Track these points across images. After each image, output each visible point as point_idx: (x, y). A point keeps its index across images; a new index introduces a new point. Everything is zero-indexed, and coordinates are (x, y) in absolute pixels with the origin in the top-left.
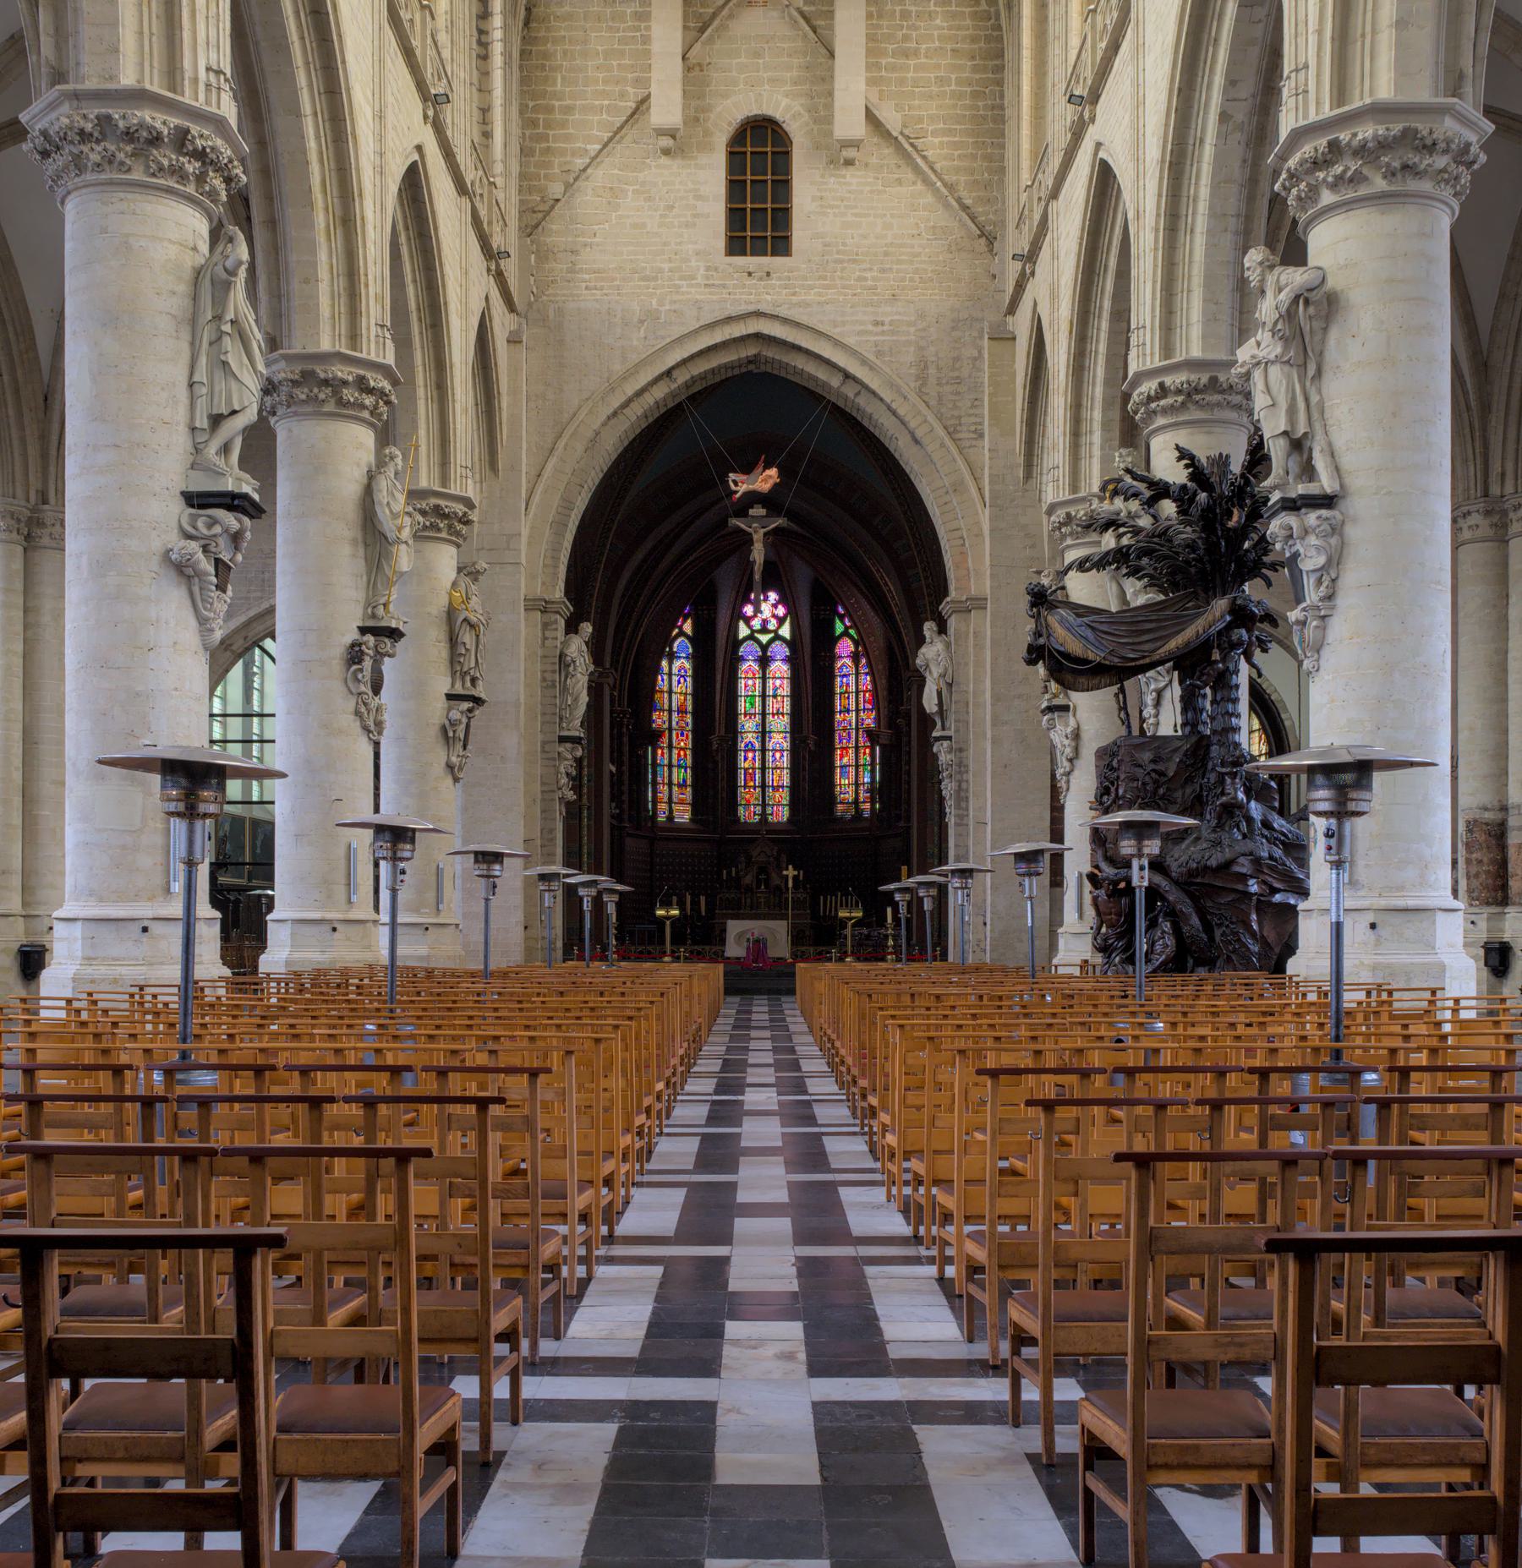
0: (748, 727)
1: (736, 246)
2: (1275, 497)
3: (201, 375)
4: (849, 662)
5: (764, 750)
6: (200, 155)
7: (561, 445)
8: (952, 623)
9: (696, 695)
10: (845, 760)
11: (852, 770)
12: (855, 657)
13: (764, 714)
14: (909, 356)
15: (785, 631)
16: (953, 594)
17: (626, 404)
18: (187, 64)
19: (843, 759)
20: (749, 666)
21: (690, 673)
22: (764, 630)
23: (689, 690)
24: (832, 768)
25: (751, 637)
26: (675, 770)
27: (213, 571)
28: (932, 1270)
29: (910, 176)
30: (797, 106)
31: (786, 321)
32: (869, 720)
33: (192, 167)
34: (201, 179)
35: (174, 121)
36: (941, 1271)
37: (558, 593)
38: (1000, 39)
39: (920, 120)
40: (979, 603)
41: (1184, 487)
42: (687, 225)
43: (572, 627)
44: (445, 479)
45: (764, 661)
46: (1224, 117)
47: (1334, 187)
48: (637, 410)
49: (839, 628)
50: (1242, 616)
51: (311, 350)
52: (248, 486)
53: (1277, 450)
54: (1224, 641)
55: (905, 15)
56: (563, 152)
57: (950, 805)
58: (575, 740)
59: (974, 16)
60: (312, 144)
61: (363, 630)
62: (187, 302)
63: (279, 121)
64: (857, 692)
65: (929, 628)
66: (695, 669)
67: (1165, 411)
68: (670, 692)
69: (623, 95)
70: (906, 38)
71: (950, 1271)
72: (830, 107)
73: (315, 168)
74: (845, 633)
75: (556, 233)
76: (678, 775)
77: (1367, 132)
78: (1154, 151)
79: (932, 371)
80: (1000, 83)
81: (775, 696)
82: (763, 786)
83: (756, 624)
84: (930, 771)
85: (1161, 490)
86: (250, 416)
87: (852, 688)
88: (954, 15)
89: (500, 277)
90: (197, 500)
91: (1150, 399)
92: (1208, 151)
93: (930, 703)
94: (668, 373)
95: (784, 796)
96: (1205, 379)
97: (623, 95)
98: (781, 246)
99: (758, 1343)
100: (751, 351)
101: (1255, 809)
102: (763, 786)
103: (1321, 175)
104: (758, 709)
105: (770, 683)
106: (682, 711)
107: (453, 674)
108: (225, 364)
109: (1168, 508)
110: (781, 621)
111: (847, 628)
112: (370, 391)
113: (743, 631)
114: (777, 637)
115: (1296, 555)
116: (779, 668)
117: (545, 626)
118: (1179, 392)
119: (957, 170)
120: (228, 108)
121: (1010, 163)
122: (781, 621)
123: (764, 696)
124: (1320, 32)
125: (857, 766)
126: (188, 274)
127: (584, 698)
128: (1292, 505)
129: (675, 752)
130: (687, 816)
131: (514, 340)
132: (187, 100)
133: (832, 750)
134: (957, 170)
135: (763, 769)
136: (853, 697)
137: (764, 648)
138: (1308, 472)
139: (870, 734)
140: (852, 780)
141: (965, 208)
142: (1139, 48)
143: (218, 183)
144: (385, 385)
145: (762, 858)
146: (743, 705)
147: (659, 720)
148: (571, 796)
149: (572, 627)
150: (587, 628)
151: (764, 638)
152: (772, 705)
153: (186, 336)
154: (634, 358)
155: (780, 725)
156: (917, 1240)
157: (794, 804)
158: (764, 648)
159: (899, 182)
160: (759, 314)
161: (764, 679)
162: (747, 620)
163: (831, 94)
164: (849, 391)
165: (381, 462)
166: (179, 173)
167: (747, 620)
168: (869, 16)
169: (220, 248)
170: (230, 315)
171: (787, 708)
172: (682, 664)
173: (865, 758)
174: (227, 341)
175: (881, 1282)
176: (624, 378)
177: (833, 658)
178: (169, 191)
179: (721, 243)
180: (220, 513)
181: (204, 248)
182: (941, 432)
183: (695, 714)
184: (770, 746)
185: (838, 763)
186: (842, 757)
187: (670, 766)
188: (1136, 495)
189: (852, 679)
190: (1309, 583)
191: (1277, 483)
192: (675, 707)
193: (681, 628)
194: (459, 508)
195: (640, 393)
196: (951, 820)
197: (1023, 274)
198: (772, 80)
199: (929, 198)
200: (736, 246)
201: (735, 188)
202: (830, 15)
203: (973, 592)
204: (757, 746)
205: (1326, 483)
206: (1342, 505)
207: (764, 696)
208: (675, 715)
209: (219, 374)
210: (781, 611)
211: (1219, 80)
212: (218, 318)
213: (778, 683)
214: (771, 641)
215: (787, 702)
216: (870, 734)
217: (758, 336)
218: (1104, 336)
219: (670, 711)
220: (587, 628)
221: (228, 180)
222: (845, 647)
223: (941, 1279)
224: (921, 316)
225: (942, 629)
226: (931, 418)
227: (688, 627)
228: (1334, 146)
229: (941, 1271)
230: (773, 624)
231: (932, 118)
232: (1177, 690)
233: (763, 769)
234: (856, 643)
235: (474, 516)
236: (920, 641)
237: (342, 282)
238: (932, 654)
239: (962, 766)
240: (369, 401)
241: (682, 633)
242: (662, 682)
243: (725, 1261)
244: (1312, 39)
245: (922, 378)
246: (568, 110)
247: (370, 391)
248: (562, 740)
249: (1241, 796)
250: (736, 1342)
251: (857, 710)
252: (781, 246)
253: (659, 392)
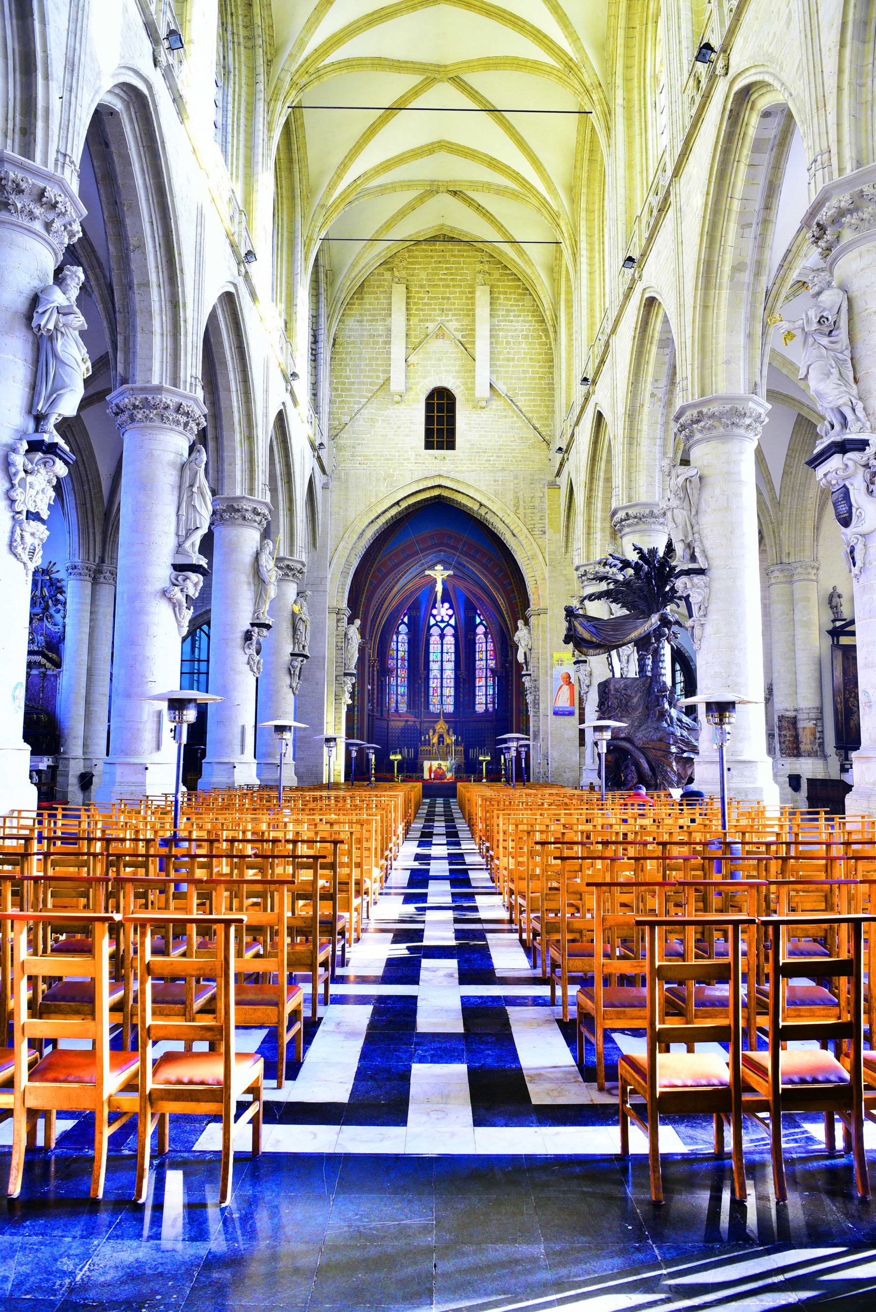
0: (434, 667)
1: (429, 446)
2: (678, 570)
3: (183, 511)
5: (442, 678)
6: (187, 414)
7: (346, 536)
8: (533, 620)
9: (409, 652)
12: (486, 634)
13: (442, 661)
14: (510, 496)
15: (452, 622)
16: (533, 607)
17: (377, 517)
18: (182, 375)
19: (480, 683)
20: (434, 639)
22: (442, 621)
24: (475, 687)
25: (436, 625)
27: (184, 600)
28: (517, 936)
29: (511, 414)
30: (458, 382)
31: (453, 480)
32: (492, 664)
33: (183, 419)
34: (186, 424)
35: (177, 400)
36: (521, 936)
37: (345, 605)
38: (552, 354)
39: (515, 389)
40: (545, 611)
41: (637, 563)
42: (407, 435)
43: (351, 621)
44: (292, 553)
45: (442, 636)
46: (653, 395)
47: (701, 431)
48: (383, 520)
49: (478, 620)
50: (665, 622)
51: (231, 496)
52: (203, 562)
53: (679, 548)
54: (658, 634)
55: (508, 343)
56: (349, 402)
57: (530, 706)
58: (351, 675)
59: (541, 344)
60: (235, 404)
61: (253, 625)
62: (177, 479)
63: (222, 394)
65: (520, 623)
66: (409, 640)
67: (629, 526)
68: (397, 650)
69: (378, 377)
70: (508, 353)
71: (525, 936)
72: (473, 383)
73: (236, 414)
74: (481, 623)
75: (345, 438)
76: (401, 690)
77: (715, 408)
78: (621, 409)
79: (521, 502)
80: (552, 373)
82: (442, 695)
83: (439, 618)
84: (522, 692)
85: (626, 564)
86: (204, 530)
88: (530, 343)
89: (319, 458)
90: (179, 568)
91: (622, 520)
92: (646, 410)
93: (521, 658)
94: (397, 503)
95: (451, 700)
96: (647, 511)
97: (378, 377)
98: (451, 446)
99: (434, 970)
100: (436, 492)
101: (674, 713)
102: (442, 695)
103: (695, 426)
104: (439, 659)
106: (403, 659)
107: (294, 644)
108: (194, 506)
109: (630, 571)
110: (450, 617)
112: (259, 514)
113: (432, 622)
114: (449, 625)
115: (689, 596)
116: (450, 640)
117: (338, 620)
118: (635, 517)
119: (532, 412)
120: (200, 394)
121: (557, 408)
122: (450, 617)
123: (442, 652)
124: (692, 365)
126: (178, 466)
127: (356, 655)
128: (688, 572)
131: (325, 487)
132: (181, 390)
133: (475, 678)
134: (532, 412)
135: (442, 687)
137: (442, 630)
138: (693, 558)
139: (492, 670)
141: (535, 428)
142: (614, 364)
143: (193, 425)
144: (267, 512)
146: (432, 657)
147: (391, 663)
148: (350, 702)
149: (351, 621)
150: (358, 622)
151: (442, 625)
153: (176, 494)
154: (381, 496)
155: (449, 666)
156: (511, 921)
157: (456, 704)
158: (442, 630)
159: (505, 417)
160: (440, 476)
161: (442, 644)
162: (434, 616)
163: (474, 377)
164: (483, 511)
165: (262, 547)
166: (178, 423)
167: (434, 616)
168: (491, 343)
169: (193, 455)
170: (197, 485)
171: (453, 659)
172: (403, 637)
173: (490, 683)
174: (195, 496)
175: (494, 942)
176: (376, 505)
177: (475, 634)
178: (172, 430)
179: (423, 444)
180: (190, 574)
181: (186, 454)
182: (526, 531)
183: (409, 661)
187: (397, 686)
188: (615, 566)
190: (695, 609)
191: (680, 562)
194: (299, 566)
195: (384, 512)
196: (531, 714)
197: (563, 459)
198: (447, 371)
199: (520, 424)
200: (429, 446)
201: (429, 420)
202: (473, 343)
203: (542, 606)
205: (701, 563)
206: (709, 573)
207: (442, 652)
209: (191, 510)
210: (450, 612)
211: (650, 379)
212: (192, 486)
216: (492, 670)
217: (439, 486)
218: (601, 489)
220: (358, 622)
221: (198, 424)
222: (480, 630)
223: (521, 940)
224: (516, 477)
225: (527, 623)
226: (521, 525)
227: (406, 620)
228: (700, 413)
229: (521, 936)
230: (446, 618)
231: (520, 389)
232: (636, 656)
233: (442, 687)
234: (486, 628)
235: (305, 570)
236: (517, 629)
237: (247, 465)
238: (521, 636)
239: (537, 689)
240: (258, 518)
241: (403, 622)
242: (393, 645)
243: (423, 930)
244: (689, 367)
245: (517, 506)
246: (353, 383)
247: (259, 514)
248: (346, 674)
249: (667, 706)
250: (427, 969)
252: (451, 446)
253: (394, 512)
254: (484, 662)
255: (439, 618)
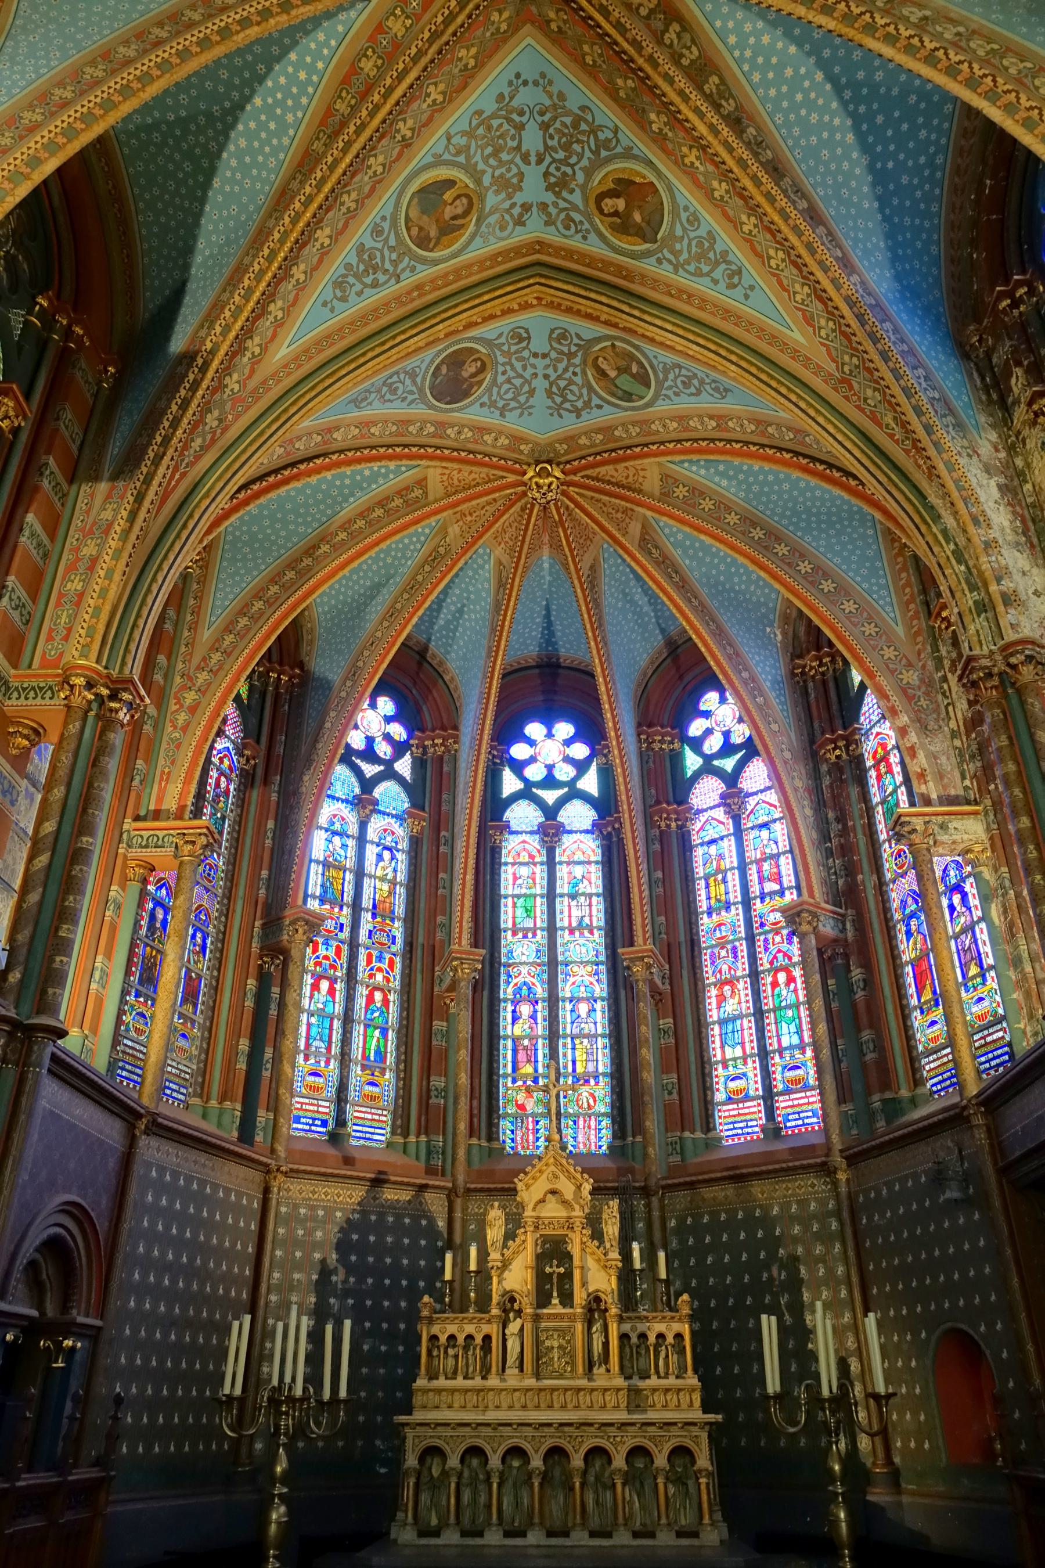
4: (720, 813)
5: (553, 1000)
10: (730, 1007)
11: (749, 1025)
13: (552, 929)
21: (404, 845)
22: (550, 781)
23: (401, 877)
26: (358, 1031)
49: (692, 762)
64: (743, 868)
68: (360, 874)
81: (573, 897)
83: (535, 773)
87: (731, 860)
105: (562, 872)
110: (581, 767)
111: (708, 759)
113: (510, 783)
122: (581, 767)
123: (551, 896)
125: (759, 1014)
129: (362, 991)
130: (382, 1136)
136: (734, 879)
137: (551, 812)
140: (752, 1047)
145: (552, 1210)
151: (550, 796)
152: (568, 912)
158: (551, 812)
161: (551, 864)
162: (518, 767)
184: (566, 990)
185: (713, 1014)
186: (721, 999)
189: (729, 847)
192: (366, 902)
193: (389, 764)
204: (540, 991)
207: (551, 896)
208: (366, 917)
213: (578, 871)
214: (562, 802)
215: (598, 907)
219: (356, 907)
230: (565, 772)
251: (747, 903)
254: (736, 915)
255: (535, 773)
